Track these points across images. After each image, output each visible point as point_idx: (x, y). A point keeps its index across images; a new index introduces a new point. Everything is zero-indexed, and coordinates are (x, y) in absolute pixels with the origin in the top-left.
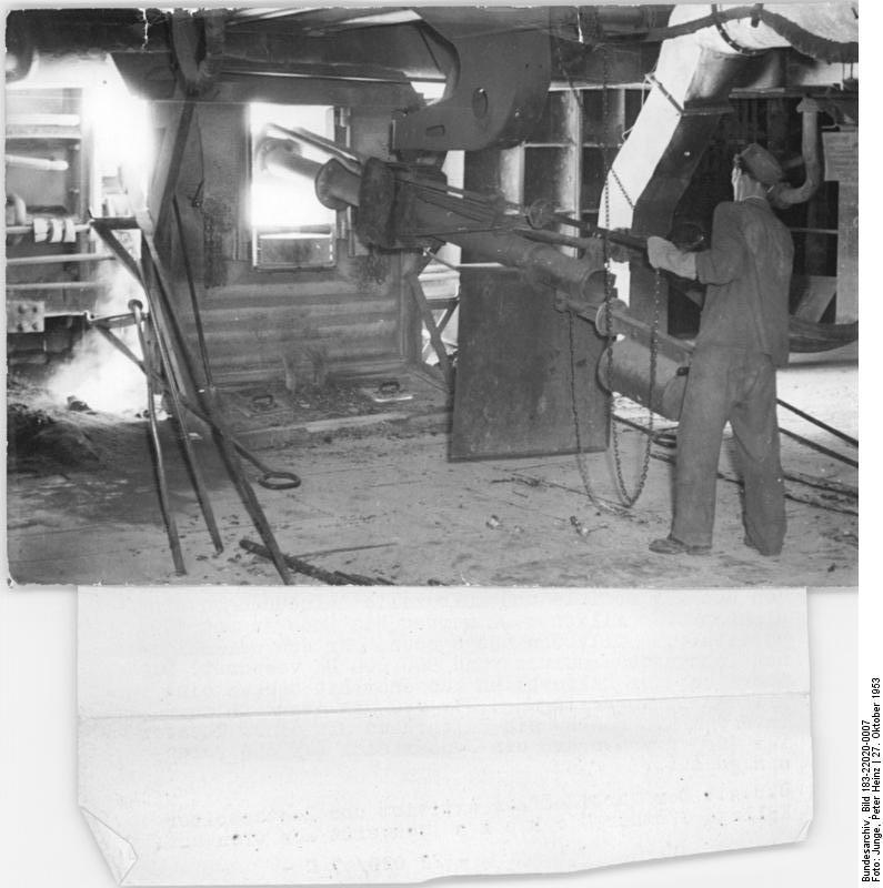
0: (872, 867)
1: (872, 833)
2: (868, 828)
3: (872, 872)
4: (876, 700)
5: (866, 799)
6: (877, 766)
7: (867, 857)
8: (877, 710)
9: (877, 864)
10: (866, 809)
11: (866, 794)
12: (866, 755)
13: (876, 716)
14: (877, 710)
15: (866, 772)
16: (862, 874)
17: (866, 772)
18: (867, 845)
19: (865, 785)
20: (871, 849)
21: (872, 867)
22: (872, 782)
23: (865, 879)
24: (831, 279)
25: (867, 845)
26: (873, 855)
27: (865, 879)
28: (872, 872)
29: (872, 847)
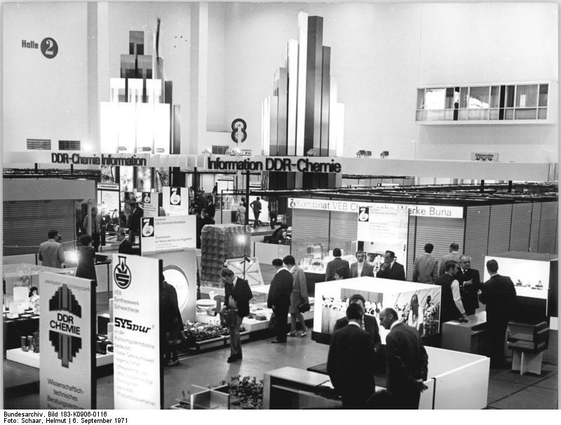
0: (14, 418)
1: (34, 418)
2: (38, 415)
3: (10, 418)
4: (114, 421)
6: (72, 421)
7: (20, 415)
8: (108, 421)
9: (15, 421)
11: (60, 414)
13: (103, 421)
14: (108, 421)
18: (27, 415)
20: (24, 417)
21: (14, 418)
25: (27, 415)
26: (19, 419)
27: (5, 414)
28: (10, 418)
29: (27, 418)
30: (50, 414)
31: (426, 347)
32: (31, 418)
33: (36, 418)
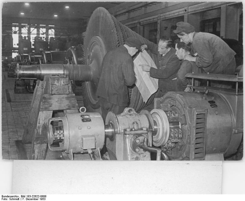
0: (6, 198)
1: (16, 198)
2: (16, 197)
3: (4, 198)
5: (25, 196)
7: (9, 196)
10: (22, 196)
12: (34, 196)
15: (32, 196)
16: (4, 195)
17: (32, 196)
18: (12, 197)
19: (28, 196)
21: (6, 198)
22: (29, 198)
23: (2, 196)
24: (223, 158)
25: (12, 197)
26: (9, 198)
27: (2, 196)
28: (4, 198)
29: (12, 198)
30: (22, 196)
31: (157, 68)
32: (14, 198)
33: (16, 198)
